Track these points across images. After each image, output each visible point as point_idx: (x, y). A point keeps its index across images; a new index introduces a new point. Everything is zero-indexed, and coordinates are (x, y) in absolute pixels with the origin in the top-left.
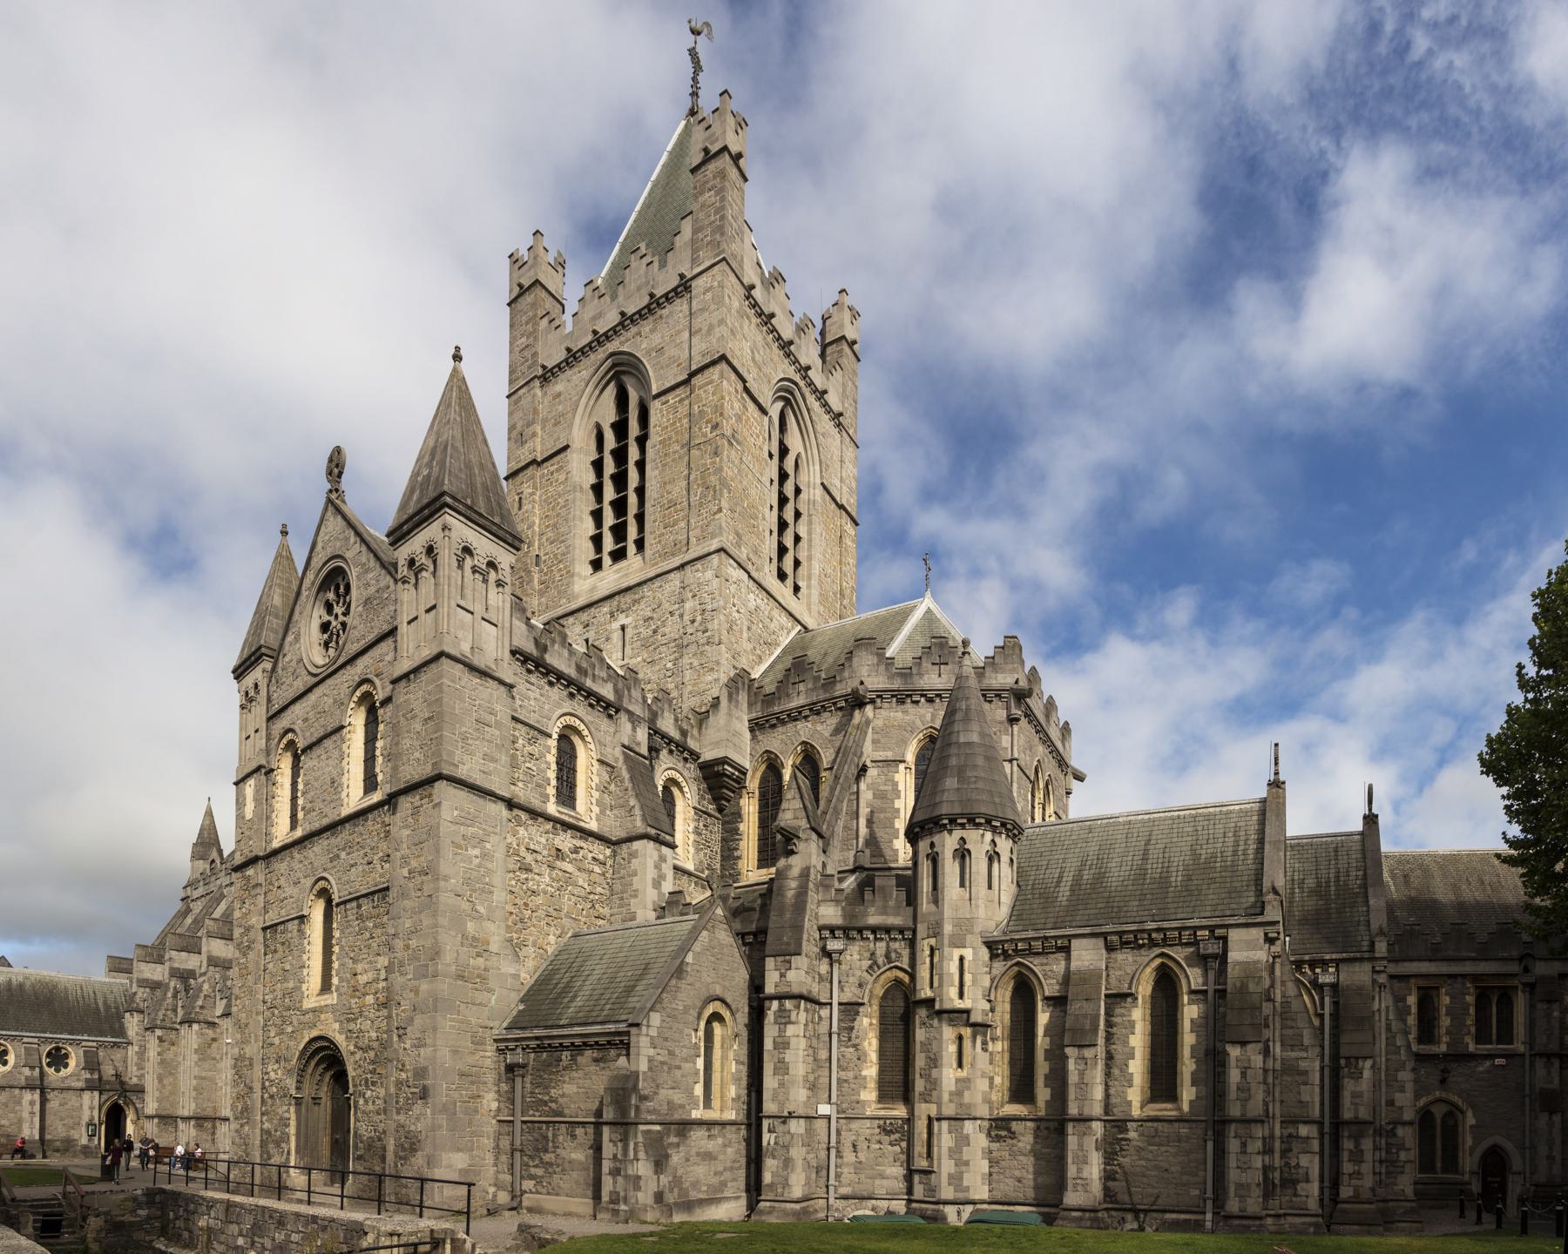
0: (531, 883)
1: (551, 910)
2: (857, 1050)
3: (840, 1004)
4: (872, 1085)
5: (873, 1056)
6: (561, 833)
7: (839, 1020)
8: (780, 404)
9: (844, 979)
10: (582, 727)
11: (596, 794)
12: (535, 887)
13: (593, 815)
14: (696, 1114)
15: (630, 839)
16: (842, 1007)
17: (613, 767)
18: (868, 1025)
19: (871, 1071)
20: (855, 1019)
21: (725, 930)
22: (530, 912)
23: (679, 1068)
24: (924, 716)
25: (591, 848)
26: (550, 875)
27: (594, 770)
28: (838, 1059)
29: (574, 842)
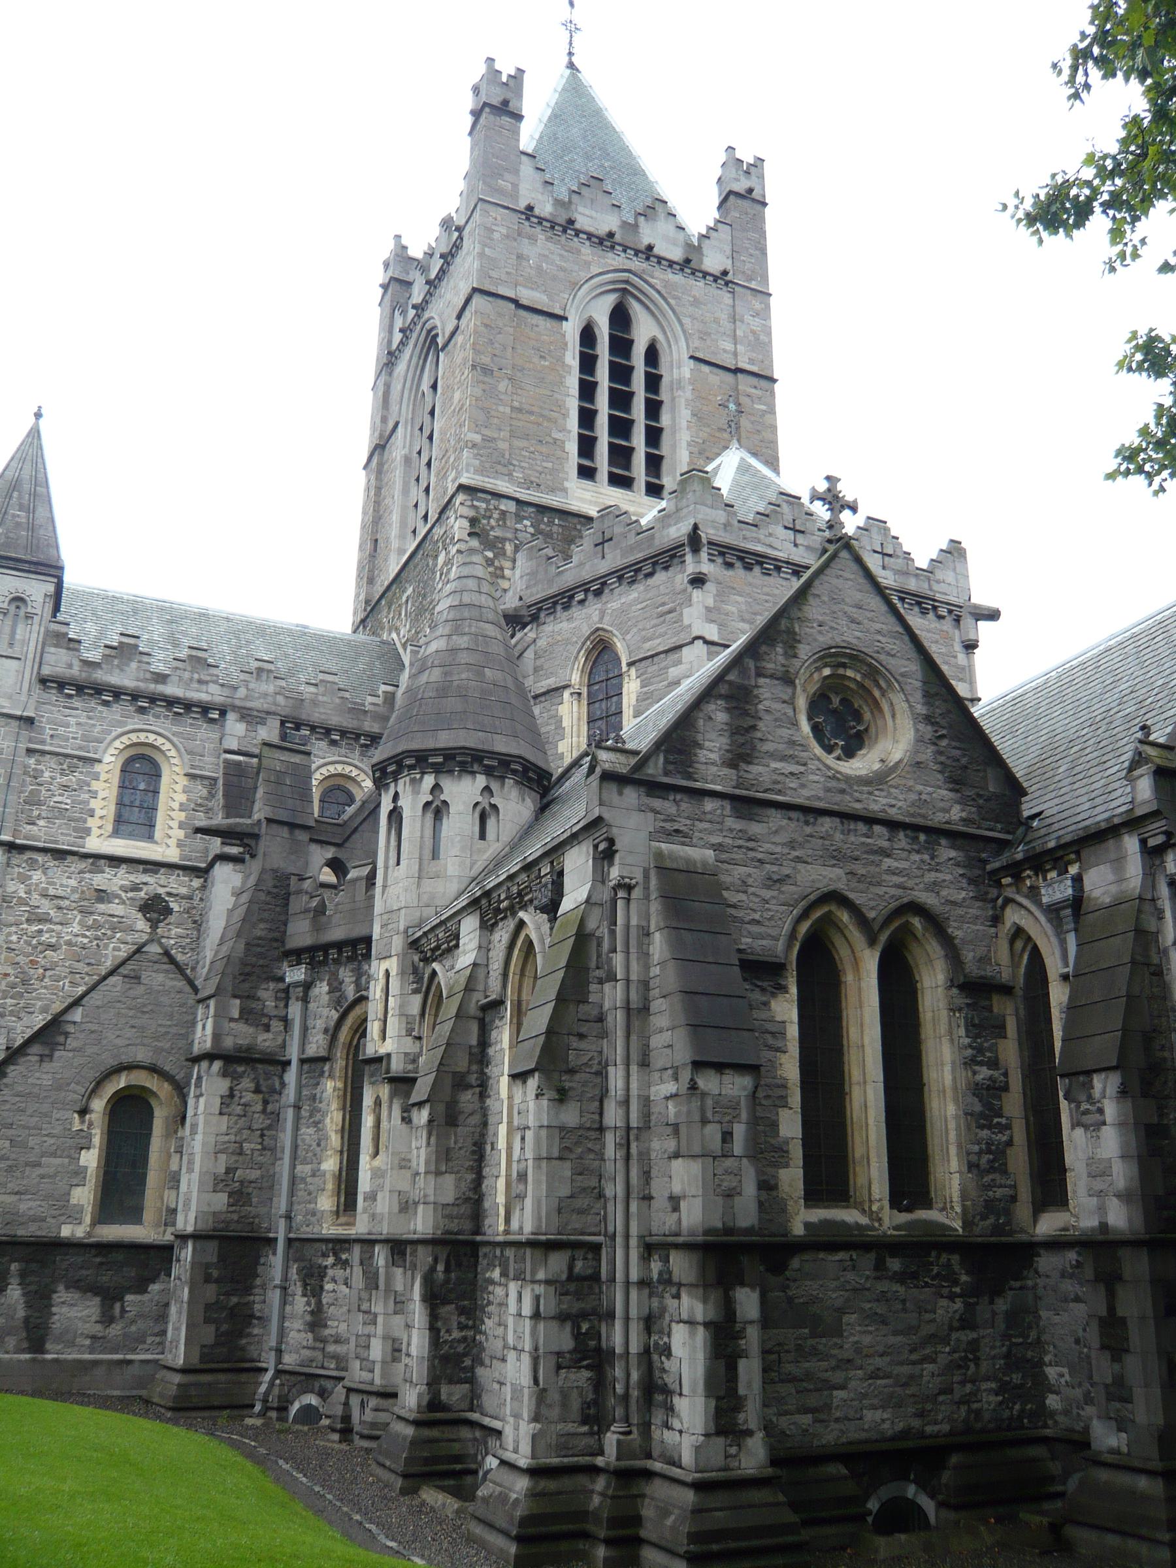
0: (47, 935)
1: (80, 966)
2: (319, 1130)
3: (303, 1061)
4: (330, 1186)
5: (335, 1140)
6: (107, 870)
7: (300, 1087)
8: (610, 300)
9: (310, 1023)
10: (151, 738)
11: (182, 816)
12: (53, 940)
13: (172, 842)
14: (66, 1232)
15: (211, 865)
16: (306, 1067)
17: (215, 779)
18: (330, 1087)
19: (331, 1165)
20: (318, 1084)
21: (167, 971)
22: (41, 971)
23: (38, 1165)
24: (589, 617)
25: (162, 882)
26: (80, 923)
27: (178, 788)
28: (295, 1147)
29: (132, 877)
